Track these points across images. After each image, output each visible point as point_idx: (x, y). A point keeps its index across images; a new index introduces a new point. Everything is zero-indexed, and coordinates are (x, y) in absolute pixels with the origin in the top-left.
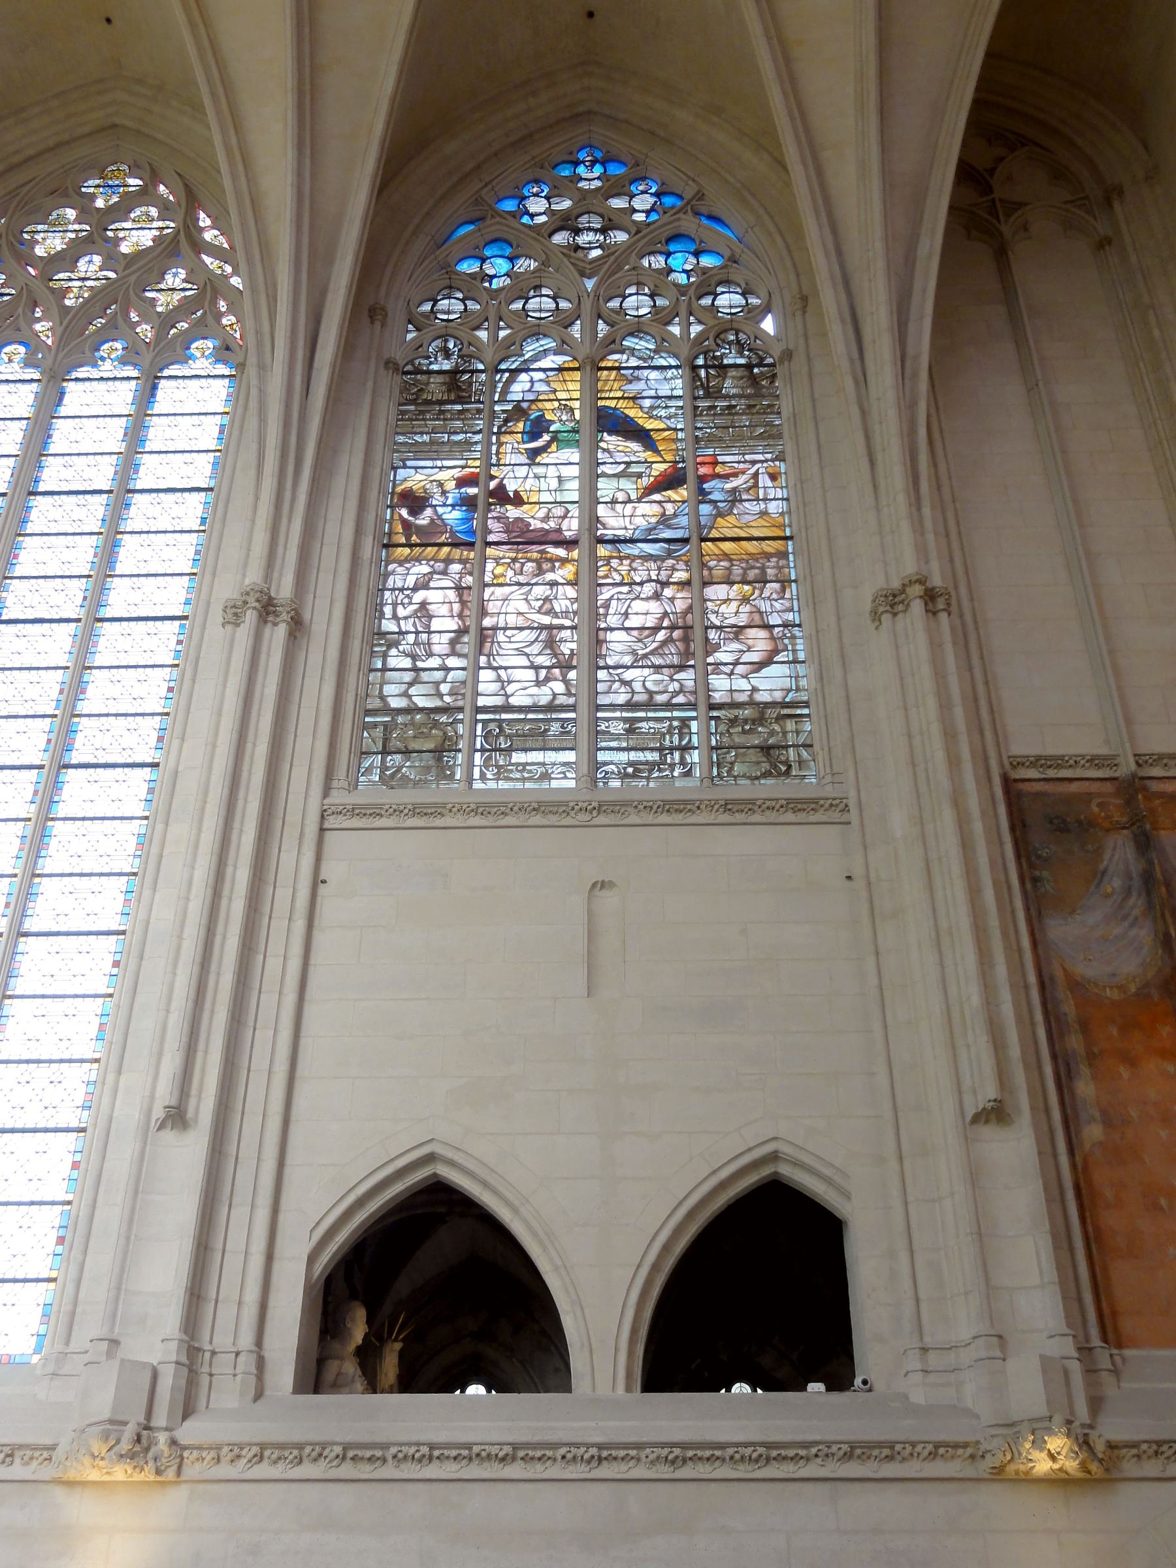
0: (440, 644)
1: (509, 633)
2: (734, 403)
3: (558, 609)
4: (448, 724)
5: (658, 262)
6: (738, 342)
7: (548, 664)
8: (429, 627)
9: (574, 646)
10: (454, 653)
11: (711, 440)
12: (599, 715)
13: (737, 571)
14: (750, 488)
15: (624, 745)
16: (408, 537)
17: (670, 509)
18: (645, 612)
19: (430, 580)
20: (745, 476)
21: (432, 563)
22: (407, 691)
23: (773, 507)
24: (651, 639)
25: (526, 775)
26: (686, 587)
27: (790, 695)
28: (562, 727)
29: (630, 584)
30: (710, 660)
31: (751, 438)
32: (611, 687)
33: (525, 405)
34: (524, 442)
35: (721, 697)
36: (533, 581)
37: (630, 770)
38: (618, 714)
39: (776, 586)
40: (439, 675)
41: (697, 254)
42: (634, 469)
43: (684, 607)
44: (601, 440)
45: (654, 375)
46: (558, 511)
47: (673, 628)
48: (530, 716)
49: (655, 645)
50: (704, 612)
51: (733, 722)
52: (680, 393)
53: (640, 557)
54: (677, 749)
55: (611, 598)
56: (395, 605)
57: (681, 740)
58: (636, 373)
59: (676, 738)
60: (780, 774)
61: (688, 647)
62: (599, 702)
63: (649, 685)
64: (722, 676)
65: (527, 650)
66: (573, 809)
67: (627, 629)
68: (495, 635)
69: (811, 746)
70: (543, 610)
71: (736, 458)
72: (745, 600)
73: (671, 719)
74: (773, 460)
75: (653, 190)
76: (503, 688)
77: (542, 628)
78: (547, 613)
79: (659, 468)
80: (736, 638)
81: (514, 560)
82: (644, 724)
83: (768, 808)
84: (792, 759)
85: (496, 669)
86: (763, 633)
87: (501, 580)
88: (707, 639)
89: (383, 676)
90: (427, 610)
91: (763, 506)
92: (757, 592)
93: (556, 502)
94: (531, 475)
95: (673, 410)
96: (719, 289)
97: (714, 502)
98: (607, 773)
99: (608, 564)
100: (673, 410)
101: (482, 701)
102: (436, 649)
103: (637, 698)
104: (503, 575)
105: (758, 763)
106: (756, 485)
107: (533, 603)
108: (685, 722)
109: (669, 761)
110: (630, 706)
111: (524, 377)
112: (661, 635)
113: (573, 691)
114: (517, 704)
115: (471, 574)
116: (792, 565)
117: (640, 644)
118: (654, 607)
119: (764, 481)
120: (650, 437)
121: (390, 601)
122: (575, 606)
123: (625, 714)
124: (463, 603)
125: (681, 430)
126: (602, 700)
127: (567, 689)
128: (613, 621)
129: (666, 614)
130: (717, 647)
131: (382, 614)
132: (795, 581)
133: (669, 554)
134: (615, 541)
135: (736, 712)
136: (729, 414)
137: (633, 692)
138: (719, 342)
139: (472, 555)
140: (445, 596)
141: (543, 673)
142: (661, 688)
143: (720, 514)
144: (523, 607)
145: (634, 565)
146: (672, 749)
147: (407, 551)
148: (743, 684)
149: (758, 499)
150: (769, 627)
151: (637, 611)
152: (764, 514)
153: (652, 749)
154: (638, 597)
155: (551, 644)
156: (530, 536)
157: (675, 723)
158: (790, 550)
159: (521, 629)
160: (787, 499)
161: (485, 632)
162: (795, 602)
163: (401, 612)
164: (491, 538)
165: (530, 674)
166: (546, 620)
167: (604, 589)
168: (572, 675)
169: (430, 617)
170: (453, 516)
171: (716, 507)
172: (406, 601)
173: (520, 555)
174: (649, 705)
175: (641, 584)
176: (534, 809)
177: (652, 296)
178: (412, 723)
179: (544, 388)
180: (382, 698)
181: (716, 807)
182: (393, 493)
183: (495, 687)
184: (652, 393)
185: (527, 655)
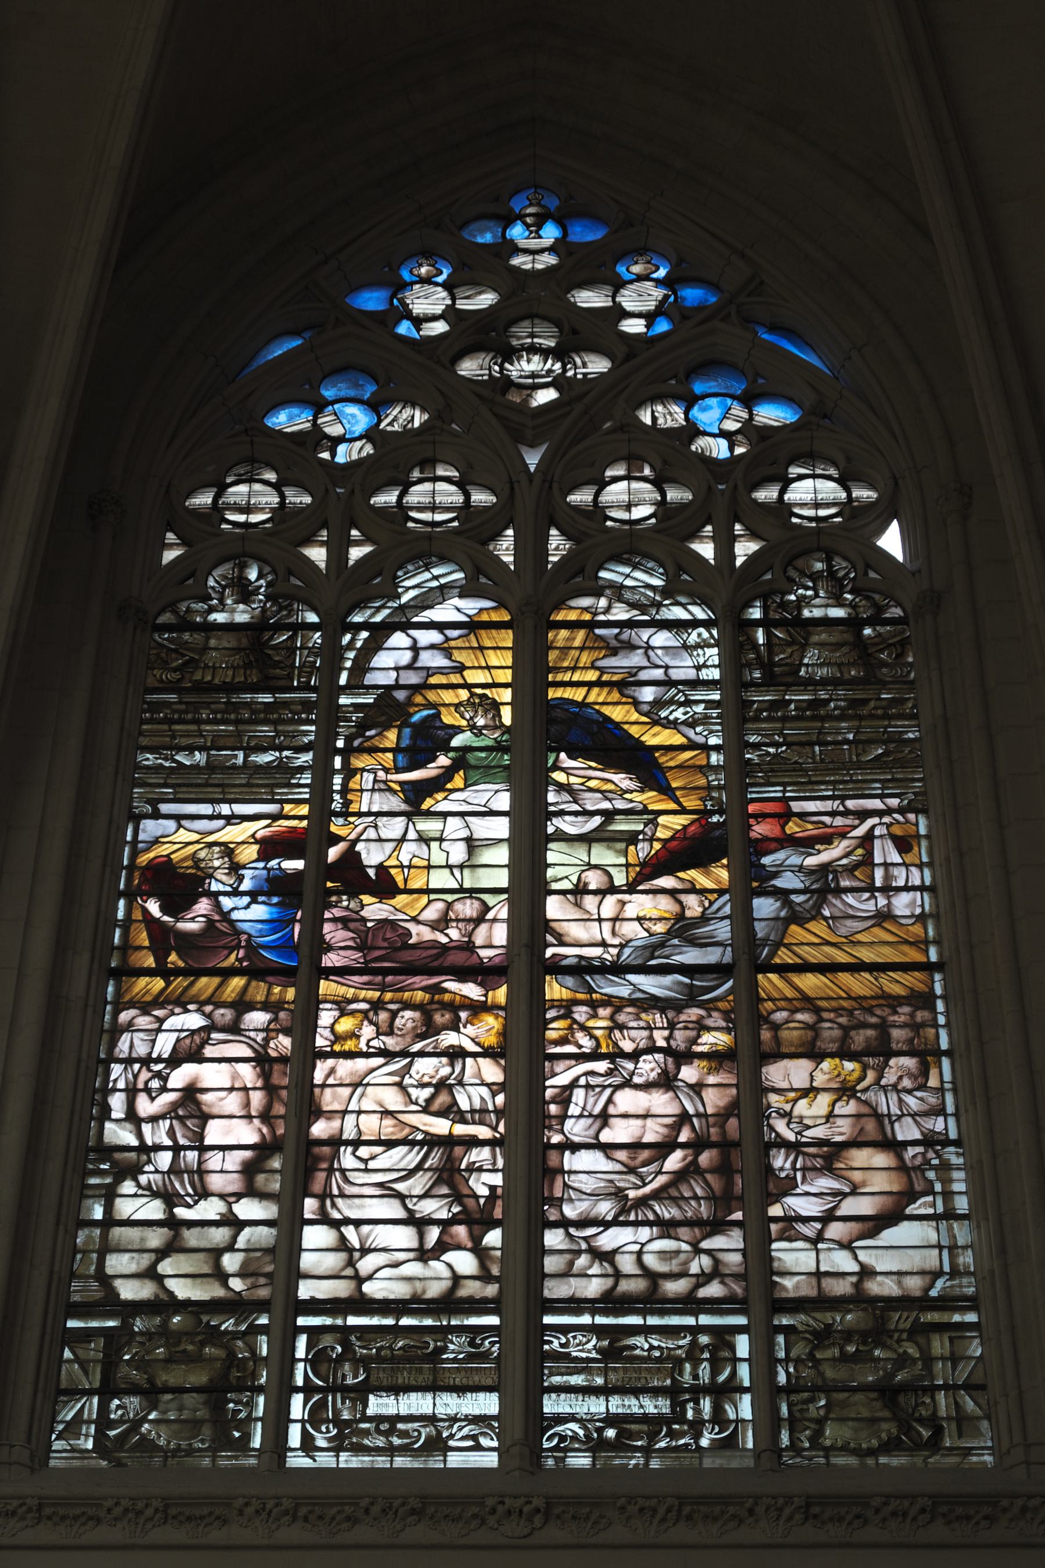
0: (224, 1171)
1: (364, 1151)
2: (823, 695)
3: (464, 1104)
4: (235, 1335)
5: (669, 415)
6: (831, 573)
7: (443, 1215)
8: (201, 1137)
9: (497, 1179)
10: (250, 1191)
11: (774, 770)
12: (548, 1320)
13: (830, 1032)
14: (856, 866)
15: (599, 1381)
16: (161, 958)
17: (693, 905)
18: (641, 1112)
19: (205, 1042)
20: (845, 843)
21: (208, 1009)
22: (153, 1266)
23: (902, 904)
25: (396, 1441)
26: (727, 1064)
27: (940, 1284)
28: (472, 1344)
29: (611, 1057)
30: (776, 1211)
31: (860, 766)
32: (571, 1264)
33: (400, 695)
34: (398, 770)
35: (797, 1287)
36: (416, 1048)
37: (611, 1433)
38: (586, 1319)
40: (219, 1235)
41: (748, 401)
42: (621, 826)
43: (722, 1103)
44: (556, 767)
45: (662, 638)
46: (468, 909)
48: (405, 1321)
49: (661, 1180)
50: (762, 1114)
51: (822, 1336)
52: (715, 674)
54: (705, 1390)
55: (574, 1084)
56: (131, 1092)
57: (715, 1372)
58: (626, 634)
59: (705, 1371)
60: (918, 1446)
61: (729, 1184)
62: (546, 1293)
63: (649, 1260)
64: (800, 1244)
65: (400, 1187)
66: (493, 1511)
67: (607, 1149)
68: (336, 1155)
69: (982, 1387)
70: (436, 1106)
71: (828, 806)
72: (846, 1091)
74: (901, 810)
75: (662, 273)
76: (351, 1263)
77: (432, 1141)
78: (441, 1114)
80: (828, 1168)
81: (377, 1005)
82: (639, 1341)
83: (894, 1514)
84: (943, 1412)
85: (336, 1225)
86: (881, 1159)
87: (349, 1045)
88: (769, 1169)
89: (104, 1236)
90: (198, 1104)
91: (882, 902)
92: (871, 1076)
93: (461, 890)
94: (412, 835)
95: (699, 709)
96: (794, 471)
98: (563, 1438)
99: (568, 1015)
100: (699, 709)
101: (306, 1290)
102: (215, 1182)
103: (624, 1286)
104: (354, 1035)
105: (873, 1421)
106: (867, 861)
107: (414, 1092)
108: (723, 1336)
109: (690, 1414)
110: (611, 1302)
111: (399, 639)
112: (674, 1161)
113: (495, 1271)
114: (379, 1296)
115: (287, 1032)
116: (941, 1020)
117: (632, 1178)
118: (661, 1102)
119: (885, 852)
121: (121, 1085)
122: (500, 1099)
123: (600, 1320)
124: (270, 1089)
125: (717, 748)
126: (555, 1290)
127: (483, 1265)
128: (576, 1129)
129: (684, 1118)
130: (788, 1187)
131: (106, 1112)
132: (946, 1053)
133: (692, 997)
134: (583, 969)
135: (828, 1317)
136: (814, 718)
137: (618, 1275)
138: (792, 573)
139: (291, 994)
140: (235, 1076)
141: (433, 1234)
142: (674, 1266)
143: (796, 917)
144: (393, 1100)
145: (621, 1018)
146: (697, 1392)
147: (159, 983)
148: (843, 1261)
149: (871, 889)
151: (622, 1113)
152: (884, 917)
153: (656, 1392)
154: (627, 1084)
155: (450, 1177)
156: (407, 956)
157: (704, 1339)
158: (938, 990)
159: (390, 1144)
160: (931, 889)
161: (316, 1150)
162: (949, 1098)
163: (145, 1106)
164: (331, 960)
165: (404, 1237)
166: (441, 1126)
167: (559, 1066)
168: (493, 1238)
169: (205, 1118)
170: (252, 915)
171: (787, 903)
172: (155, 1084)
173: (388, 996)
174: (651, 1300)
175: (635, 1056)
176: (413, 1512)
177: (658, 483)
178: (164, 1332)
179: (438, 660)
180: (105, 1280)
181: (787, 1511)
182: (132, 867)
183: (333, 1261)
184: (658, 674)
185: (401, 1197)
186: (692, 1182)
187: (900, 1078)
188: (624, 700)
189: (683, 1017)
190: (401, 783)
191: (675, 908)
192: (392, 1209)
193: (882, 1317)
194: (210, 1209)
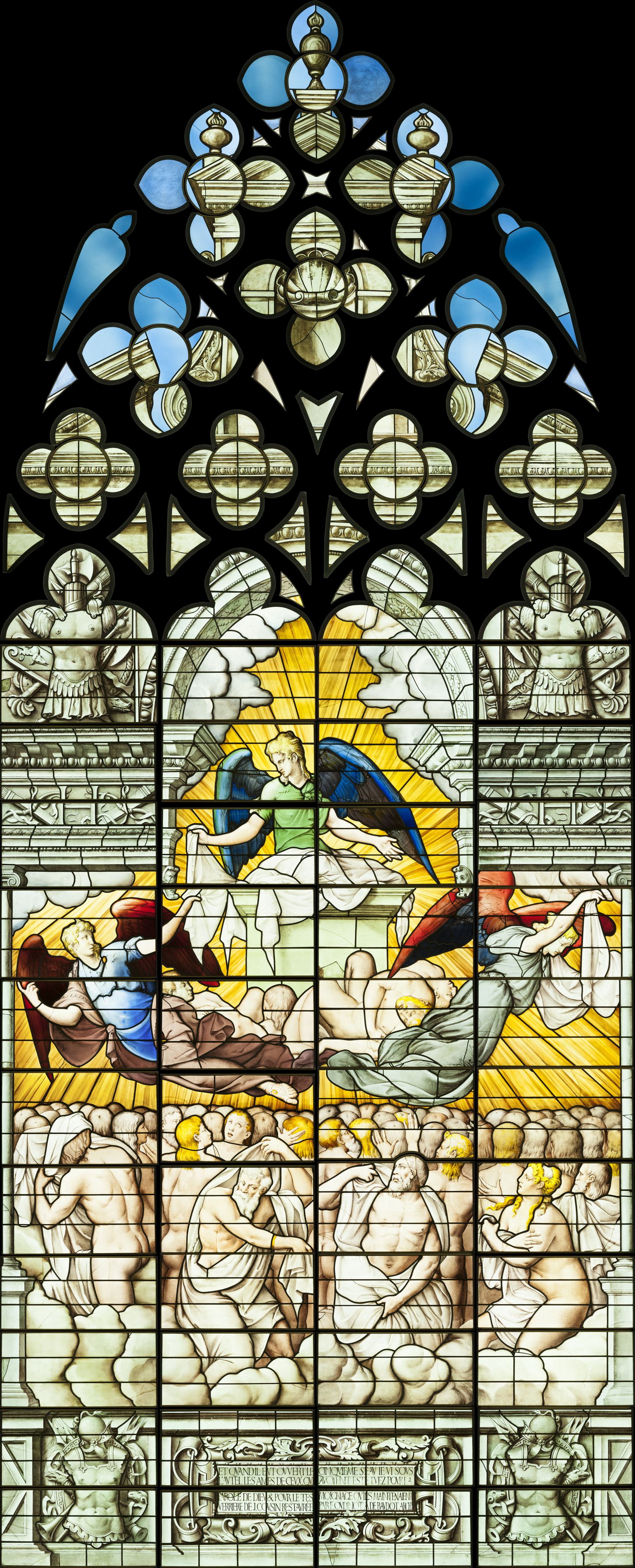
18: (399, 1219)
24: (406, 1275)
39: (597, 1169)
42: (386, 899)
47: (441, 1254)
49: (413, 1286)
53: (390, 1100)
68: (184, 1264)
72: (546, 1198)
73: (433, 1433)
79: (427, 898)
85: (186, 1332)
92: (566, 1181)
97: (505, 980)
118: (412, 1209)
120: (410, 825)
134: (357, 1064)
150: (578, 1255)
186: (435, 1288)
187: (588, 1185)
188: (388, 741)
189: (430, 1118)
190: (221, 847)
191: (428, 997)
192: (226, 1317)
193: (561, 1422)
194: (103, 1317)
